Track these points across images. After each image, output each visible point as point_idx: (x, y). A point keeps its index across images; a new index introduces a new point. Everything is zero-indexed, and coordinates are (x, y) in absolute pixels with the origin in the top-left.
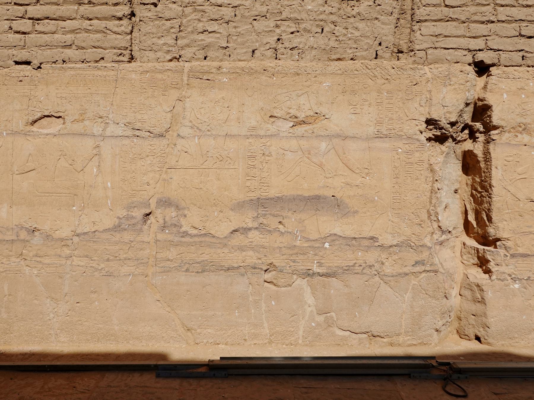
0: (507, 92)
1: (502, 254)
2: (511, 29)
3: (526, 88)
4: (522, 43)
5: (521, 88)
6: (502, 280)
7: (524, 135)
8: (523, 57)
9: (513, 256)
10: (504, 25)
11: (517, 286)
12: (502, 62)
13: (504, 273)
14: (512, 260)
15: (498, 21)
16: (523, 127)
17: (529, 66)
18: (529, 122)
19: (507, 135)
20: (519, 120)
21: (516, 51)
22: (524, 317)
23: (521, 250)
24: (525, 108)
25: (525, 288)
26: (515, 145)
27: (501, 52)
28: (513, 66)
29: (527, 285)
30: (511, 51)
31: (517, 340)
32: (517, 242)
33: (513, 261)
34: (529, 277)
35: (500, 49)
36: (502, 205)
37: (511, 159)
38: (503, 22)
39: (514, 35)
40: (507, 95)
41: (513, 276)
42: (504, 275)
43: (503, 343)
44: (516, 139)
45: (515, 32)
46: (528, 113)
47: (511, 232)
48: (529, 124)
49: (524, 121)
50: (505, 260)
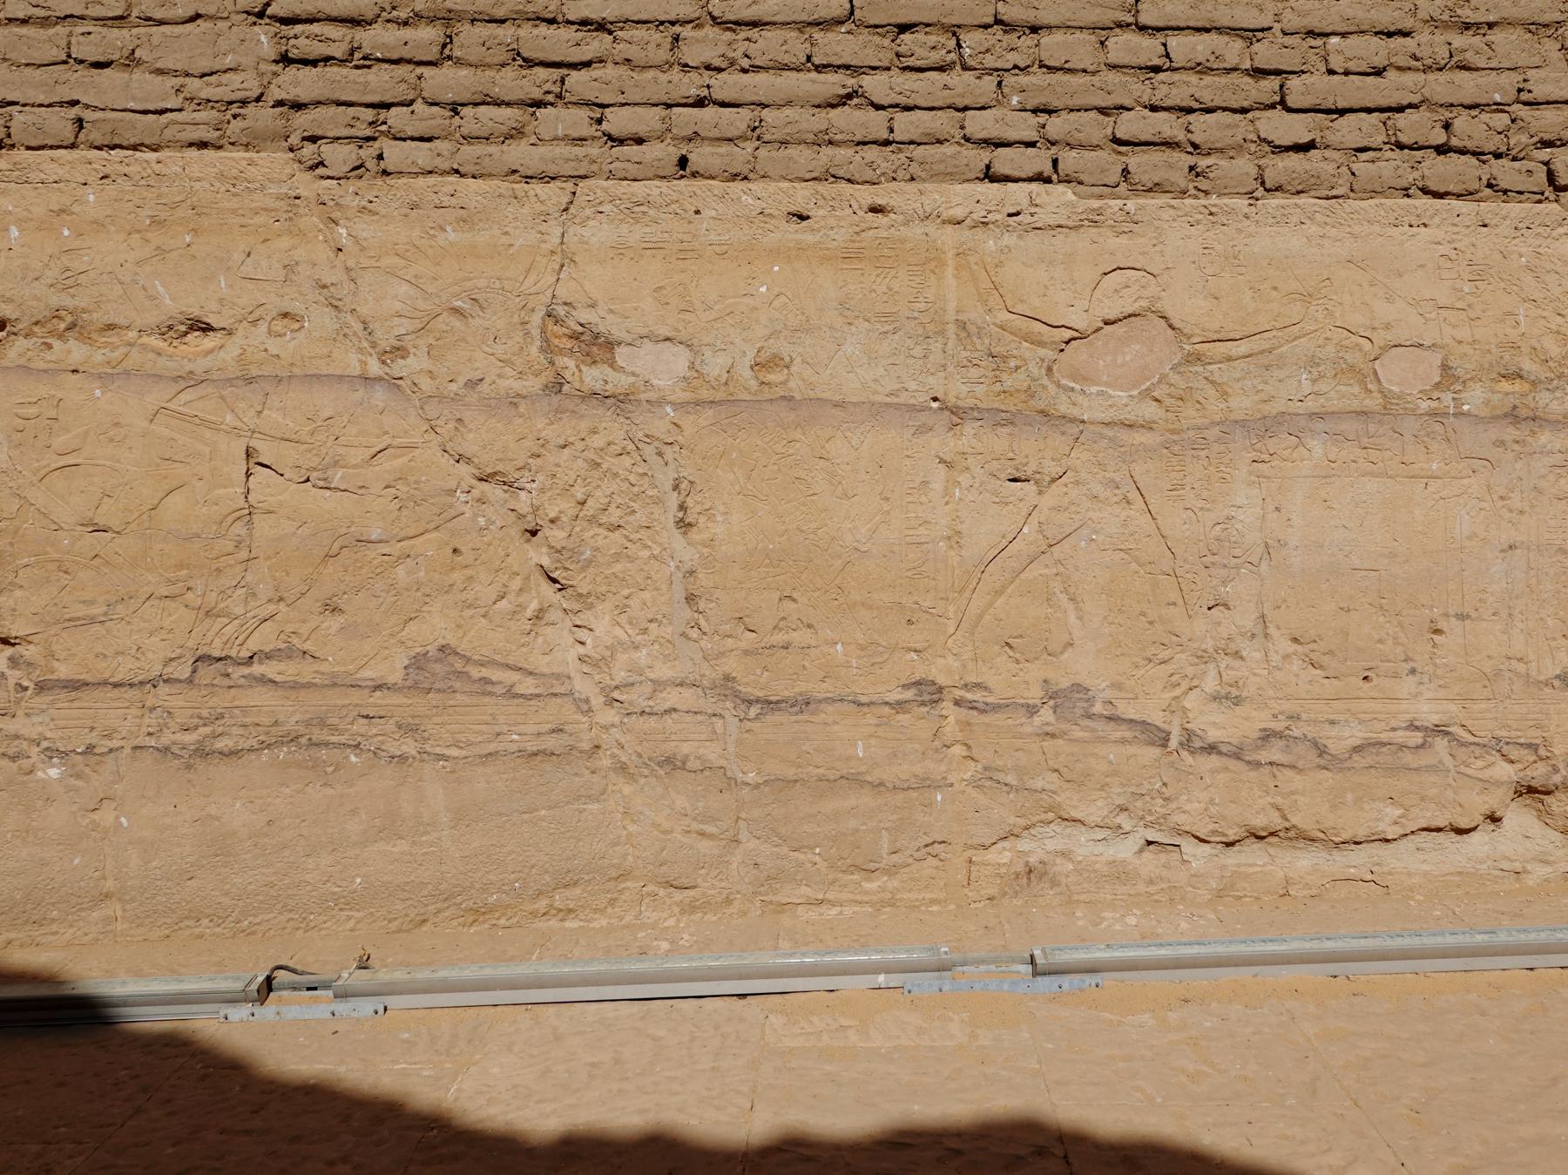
0: (20, 222)
1: (11, 682)
2: (46, 43)
3: (76, 208)
4: (77, 83)
5: (63, 211)
6: (13, 758)
7: (72, 342)
8: (80, 122)
9: (41, 687)
10: (24, 30)
11: (54, 773)
12: (15, 138)
13: (17, 737)
14: (37, 699)
15: (10, 20)
16: (69, 319)
17: (99, 148)
18: (83, 305)
19: (21, 343)
20: (55, 300)
21: (61, 104)
22: (77, 861)
23: (63, 671)
24: (78, 265)
25: (78, 776)
26: (45, 371)
27: (18, 108)
28: (51, 147)
29: (87, 770)
30: (41, 105)
31: (54, 927)
32: (54, 647)
33: (43, 700)
34: (90, 749)
35: (10, 98)
36: (11, 544)
37: (33, 410)
38: (24, 22)
39: (52, 59)
40: (21, 230)
41: (45, 744)
42: (16, 742)
43: (13, 935)
44: (49, 356)
45: (54, 51)
46: (82, 279)
47: (36, 618)
48: (84, 311)
49: (69, 303)
50: (18, 702)
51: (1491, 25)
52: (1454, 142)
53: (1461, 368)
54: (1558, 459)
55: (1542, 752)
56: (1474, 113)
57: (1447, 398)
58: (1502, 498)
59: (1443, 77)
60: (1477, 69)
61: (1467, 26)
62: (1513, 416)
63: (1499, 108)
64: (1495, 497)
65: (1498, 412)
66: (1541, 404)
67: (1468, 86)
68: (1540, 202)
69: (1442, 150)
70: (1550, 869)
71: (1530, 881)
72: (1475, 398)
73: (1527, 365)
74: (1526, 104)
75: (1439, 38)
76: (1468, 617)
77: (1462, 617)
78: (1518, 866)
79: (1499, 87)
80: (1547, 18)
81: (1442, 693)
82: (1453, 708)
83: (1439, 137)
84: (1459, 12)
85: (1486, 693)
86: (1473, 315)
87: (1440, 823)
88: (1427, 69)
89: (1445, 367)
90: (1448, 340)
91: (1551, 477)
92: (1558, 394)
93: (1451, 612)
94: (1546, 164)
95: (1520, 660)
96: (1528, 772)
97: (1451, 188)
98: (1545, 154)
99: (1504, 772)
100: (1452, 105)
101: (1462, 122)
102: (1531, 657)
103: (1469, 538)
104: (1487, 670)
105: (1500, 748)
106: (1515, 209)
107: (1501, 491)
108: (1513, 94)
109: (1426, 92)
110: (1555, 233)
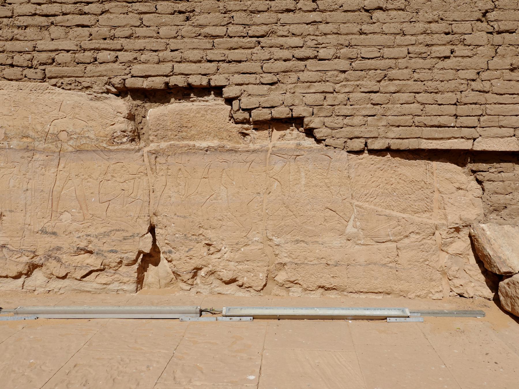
51: (26, 27)
52: (14, 64)
53: (11, 134)
54: (41, 163)
55: (37, 254)
56: (21, 54)
57: (6, 143)
58: (24, 174)
59: (10, 43)
60: (21, 40)
61: (19, 27)
62: (27, 149)
63: (28, 52)
64: (22, 174)
65: (22, 148)
66: (36, 146)
67: (18, 45)
68: (40, 82)
69: (12, 66)
70: (43, 289)
71: (36, 293)
72: (14, 143)
73: (31, 133)
74: (38, 51)
75: (10, 31)
76: (13, 211)
77: (11, 211)
78: (34, 288)
79: (27, 46)
80: (43, 24)
81: (4, 235)
82: (8, 239)
83: (9, 62)
84: (15, 22)
85: (18, 235)
86: (14, 117)
87: (4, 275)
88: (6, 40)
89: (5, 133)
90: (5, 125)
91: (40, 168)
92: (41, 142)
93: (7, 209)
94: (44, 70)
95: (29, 225)
96: (33, 259)
97: (12, 78)
98: (43, 67)
99: (25, 259)
100: (13, 52)
101: (17, 57)
102: (32, 224)
103: (14, 187)
104: (19, 228)
105: (21, 252)
106: (32, 84)
107: (24, 172)
108: (31, 49)
109: (5, 47)
110: (44, 92)
